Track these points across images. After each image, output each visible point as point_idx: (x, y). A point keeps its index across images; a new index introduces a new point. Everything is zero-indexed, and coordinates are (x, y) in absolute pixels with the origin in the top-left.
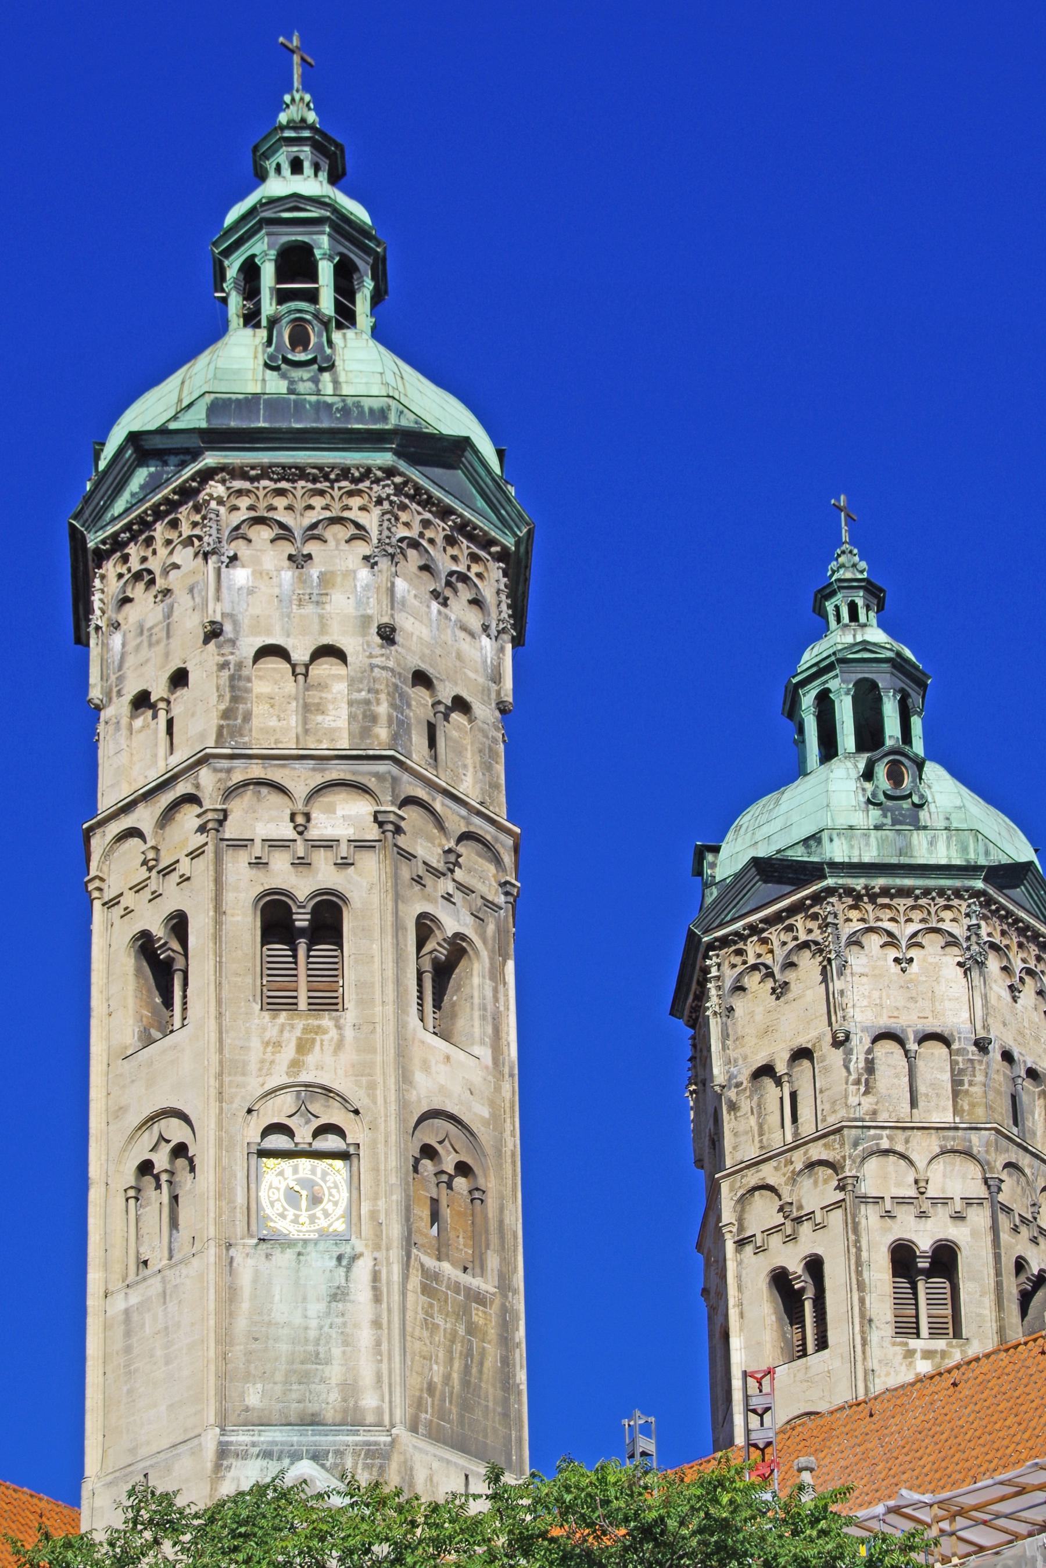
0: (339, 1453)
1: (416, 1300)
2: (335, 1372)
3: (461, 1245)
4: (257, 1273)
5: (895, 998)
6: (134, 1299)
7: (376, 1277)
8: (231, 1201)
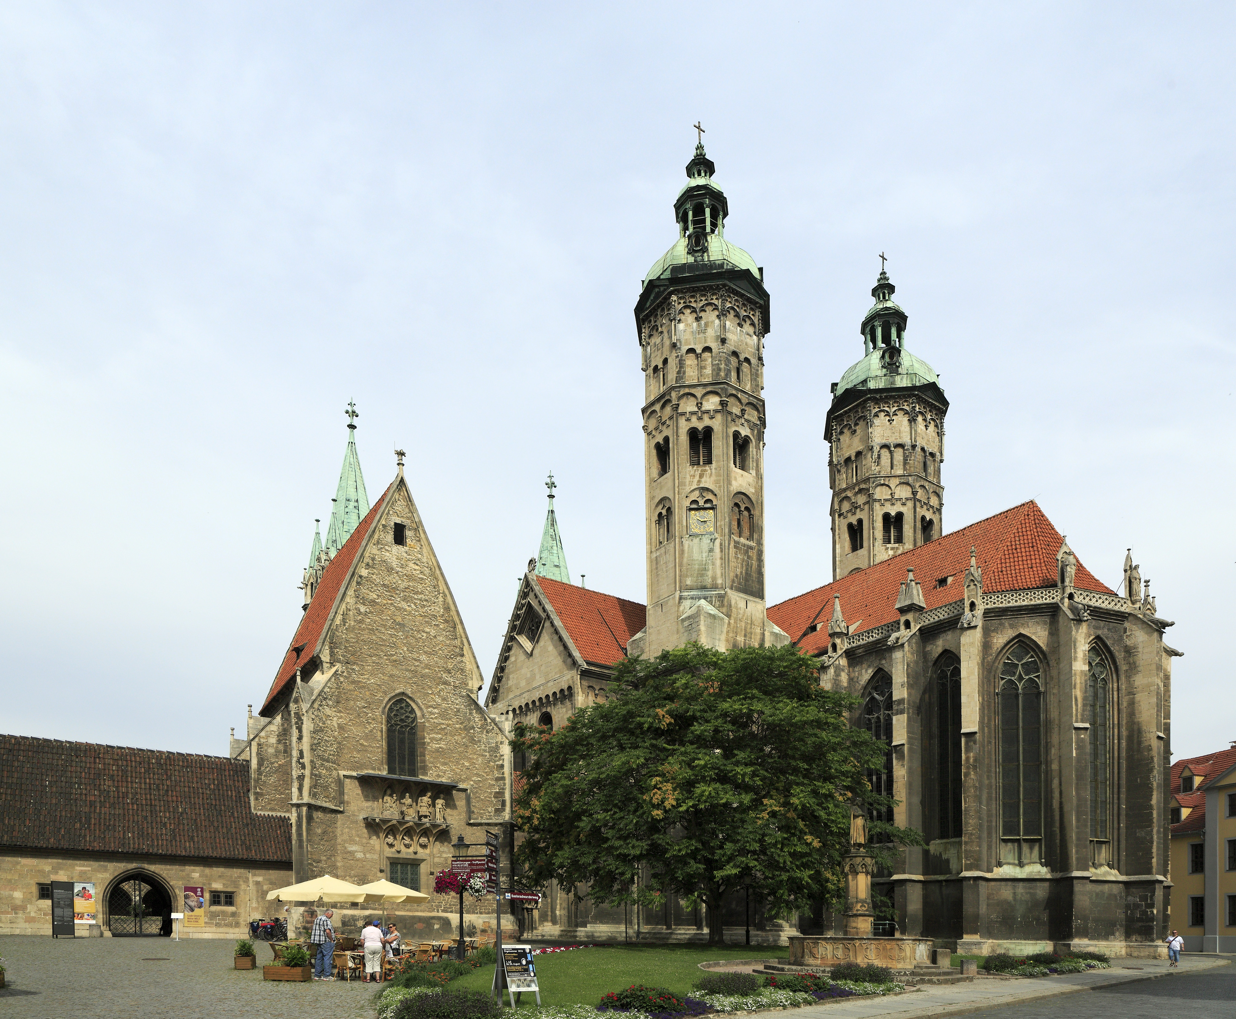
0: (711, 597)
1: (732, 550)
2: (710, 573)
3: (746, 532)
5: (888, 433)
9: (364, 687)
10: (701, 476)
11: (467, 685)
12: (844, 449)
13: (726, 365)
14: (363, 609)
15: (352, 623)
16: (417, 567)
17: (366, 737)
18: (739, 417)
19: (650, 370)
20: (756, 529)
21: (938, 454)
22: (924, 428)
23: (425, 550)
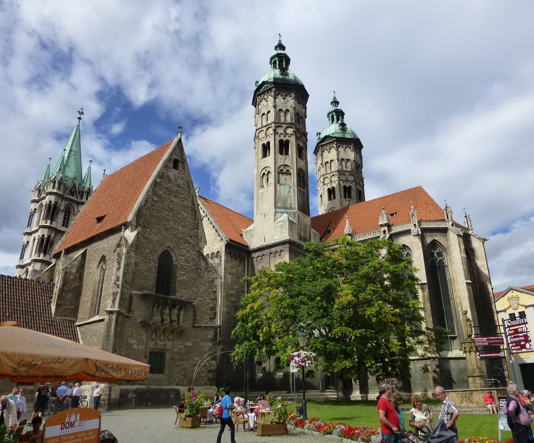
2: (289, 202)
6: (263, 191)
7: (294, 190)
10: (285, 159)
11: (199, 245)
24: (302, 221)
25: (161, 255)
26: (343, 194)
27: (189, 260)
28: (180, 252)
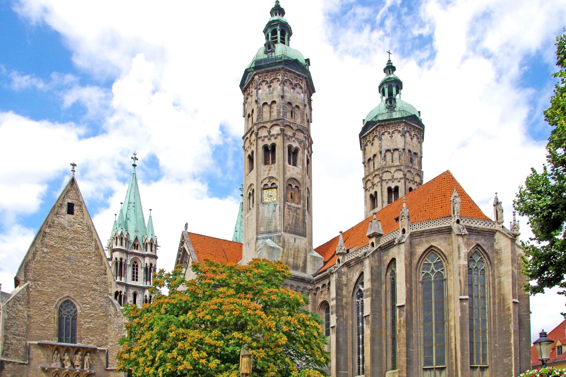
1: (286, 210)
2: (273, 224)
4: (262, 209)
8: (258, 198)
9: (44, 294)
10: (269, 170)
12: (368, 154)
13: (284, 109)
14: (45, 250)
15: (39, 258)
16: (80, 226)
17: (45, 322)
18: (292, 137)
19: (247, 116)
20: (302, 198)
21: (419, 153)
22: (410, 140)
23: (85, 216)
24: (292, 245)
25: (61, 306)
26: (386, 199)
27: (96, 308)
28: (84, 301)
